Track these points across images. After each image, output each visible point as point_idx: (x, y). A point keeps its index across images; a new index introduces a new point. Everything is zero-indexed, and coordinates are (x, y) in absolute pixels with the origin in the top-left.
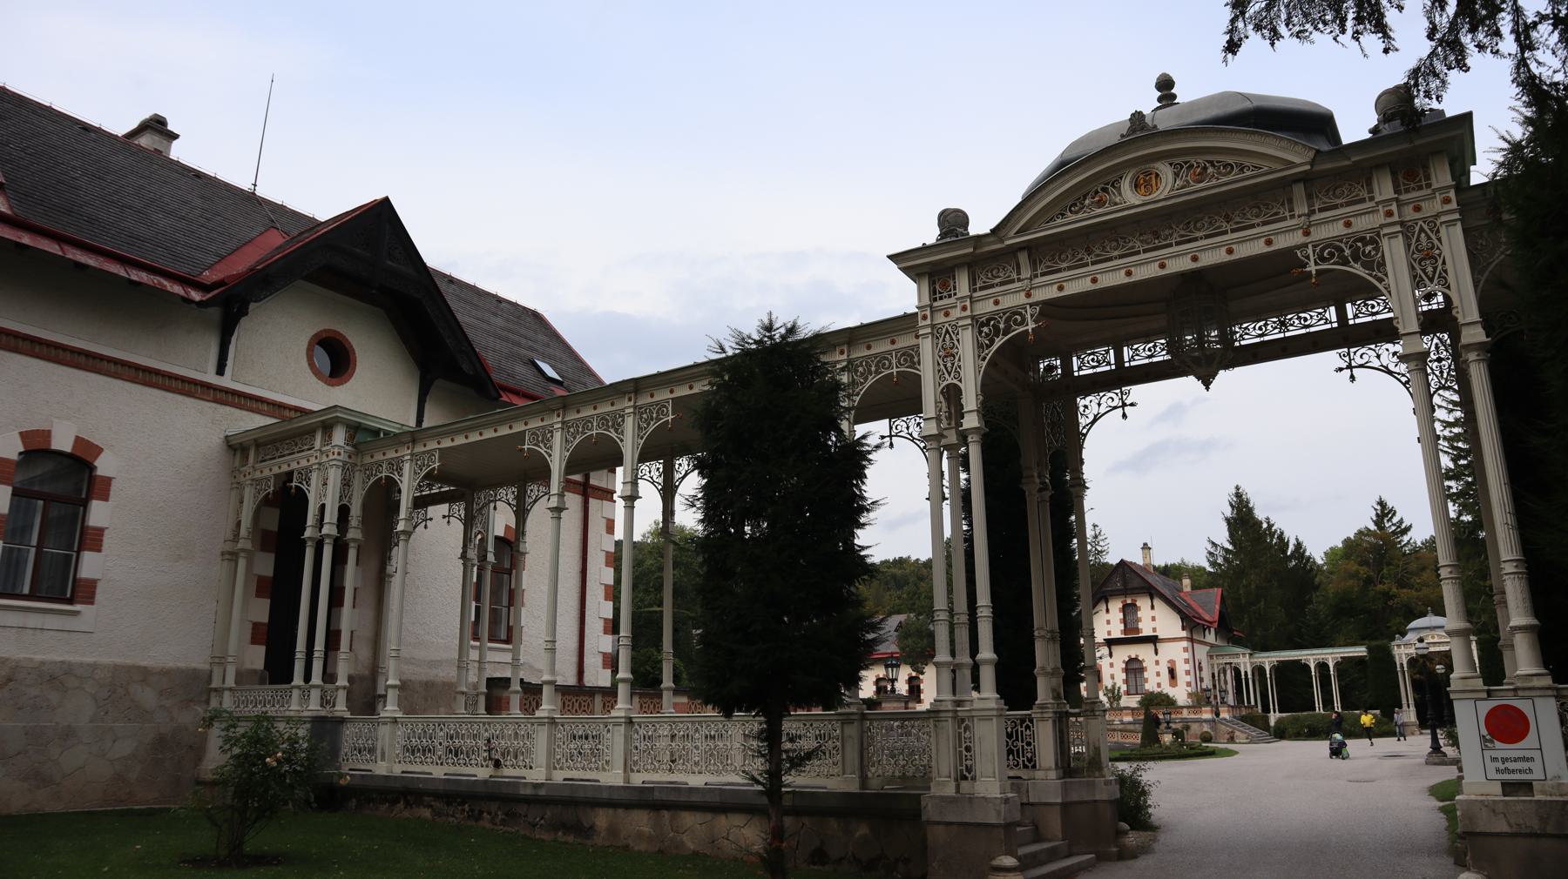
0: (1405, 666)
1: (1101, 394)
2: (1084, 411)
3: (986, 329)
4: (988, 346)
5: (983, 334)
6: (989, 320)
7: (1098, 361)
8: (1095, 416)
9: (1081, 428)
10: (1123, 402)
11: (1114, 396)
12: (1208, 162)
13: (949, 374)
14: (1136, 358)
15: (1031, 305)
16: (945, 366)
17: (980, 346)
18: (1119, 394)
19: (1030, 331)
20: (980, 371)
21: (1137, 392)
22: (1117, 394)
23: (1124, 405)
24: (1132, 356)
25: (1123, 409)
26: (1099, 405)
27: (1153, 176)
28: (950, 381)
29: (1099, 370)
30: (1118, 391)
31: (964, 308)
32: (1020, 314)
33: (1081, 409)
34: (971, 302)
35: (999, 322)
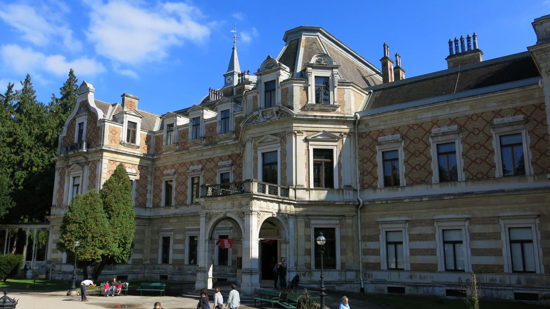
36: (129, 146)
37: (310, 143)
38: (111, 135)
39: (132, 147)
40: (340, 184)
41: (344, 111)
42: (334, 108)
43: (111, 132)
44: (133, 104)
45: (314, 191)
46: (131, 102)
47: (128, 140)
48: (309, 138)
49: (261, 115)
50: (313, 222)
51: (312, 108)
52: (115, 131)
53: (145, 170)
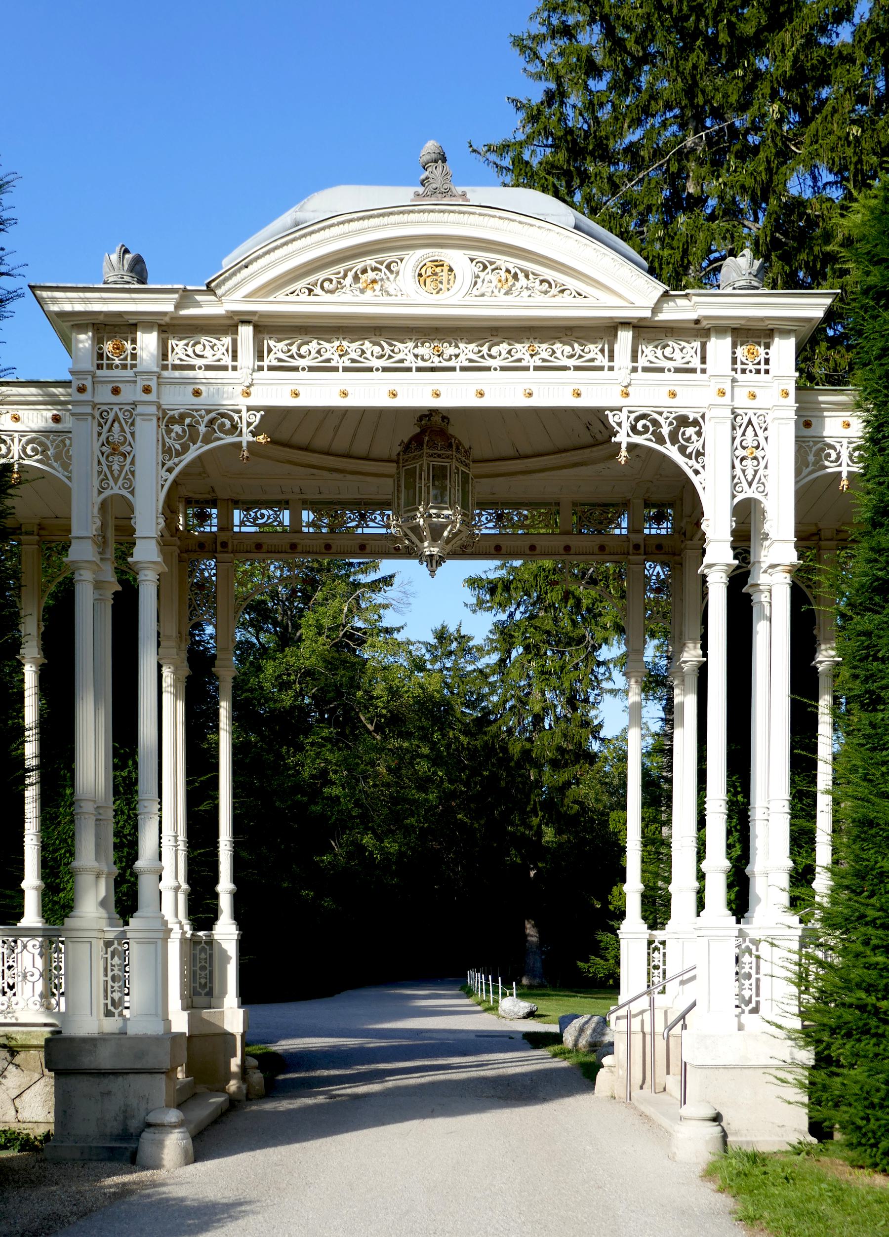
3: (177, 428)
4: (178, 454)
5: (173, 435)
6: (182, 417)
12: (522, 270)
13: (116, 481)
15: (249, 409)
16: (110, 467)
17: (167, 451)
19: (244, 444)
20: (163, 486)
27: (446, 269)
28: (116, 491)
31: (147, 390)
32: (231, 419)
34: (159, 384)
35: (198, 422)
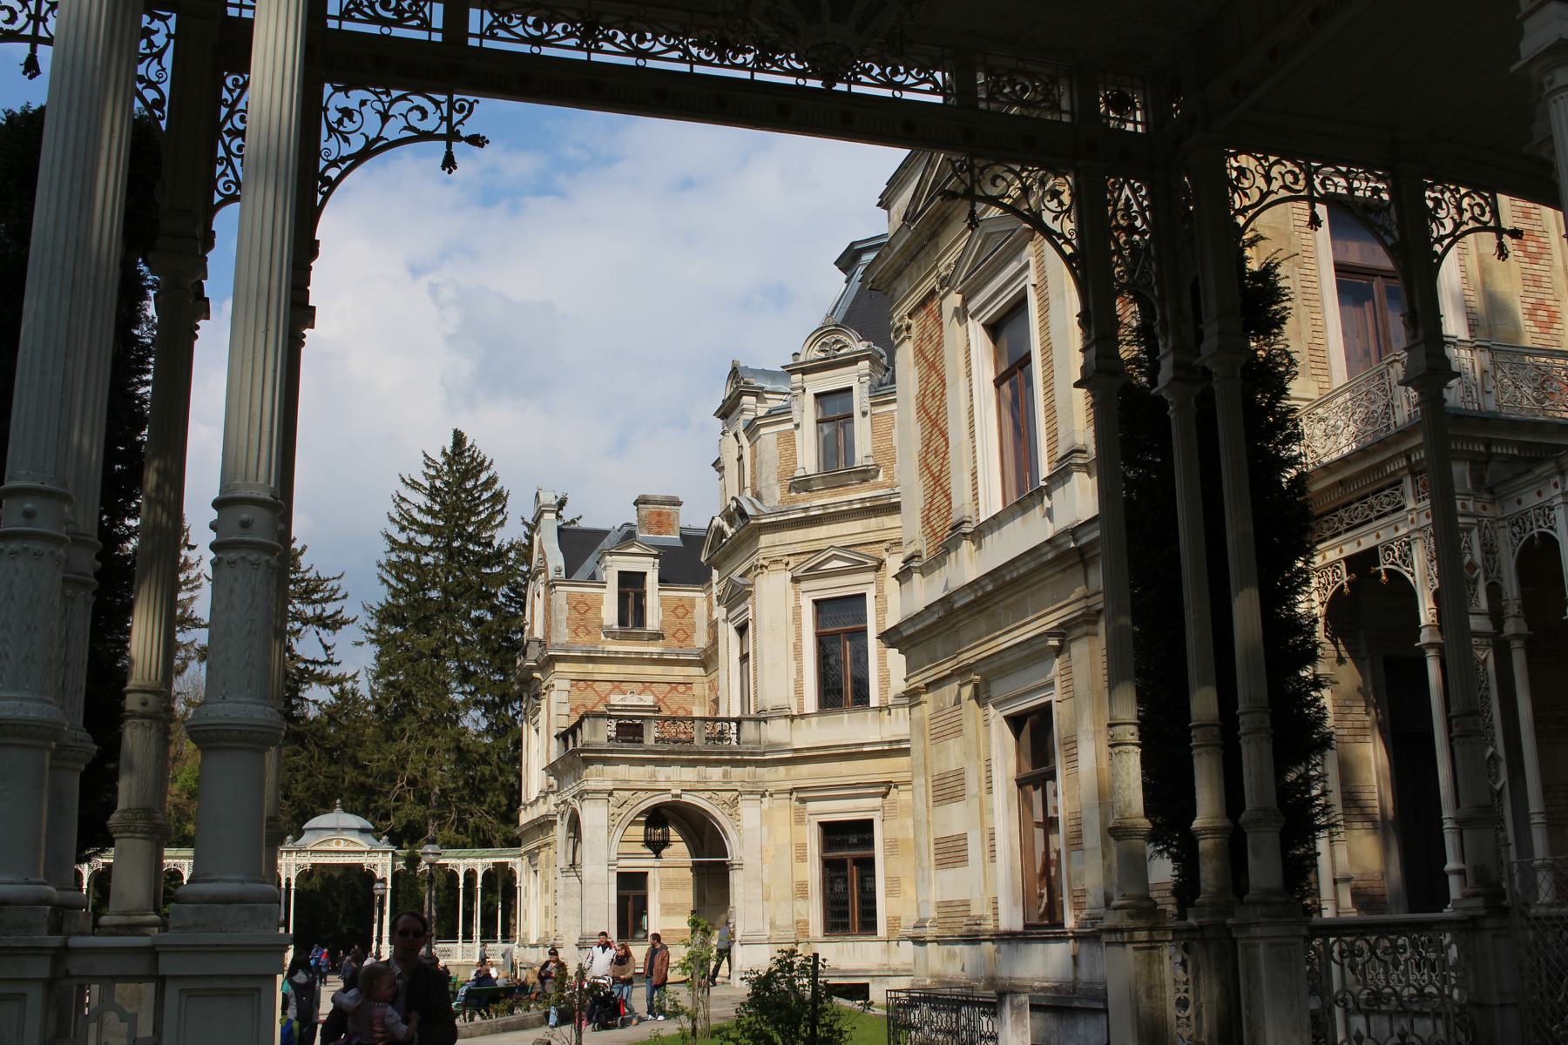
0: (293, 882)
1: (395, 93)
2: (340, 122)
7: (399, 11)
8: (369, 143)
9: (322, 164)
10: (450, 128)
11: (430, 107)
14: (502, 33)
18: (444, 107)
21: (489, 113)
22: (437, 104)
23: (452, 136)
24: (491, 27)
25: (449, 146)
26: (385, 117)
29: (397, 32)
30: (442, 98)
33: (333, 116)
36: (625, 637)
37: (804, 585)
38: (575, 615)
39: (638, 638)
40: (883, 691)
41: (892, 478)
42: (866, 475)
43: (574, 607)
44: (664, 519)
45: (814, 720)
46: (660, 514)
47: (622, 621)
48: (798, 573)
49: (726, 527)
50: (812, 806)
51: (802, 485)
52: (586, 604)
53: (684, 693)
